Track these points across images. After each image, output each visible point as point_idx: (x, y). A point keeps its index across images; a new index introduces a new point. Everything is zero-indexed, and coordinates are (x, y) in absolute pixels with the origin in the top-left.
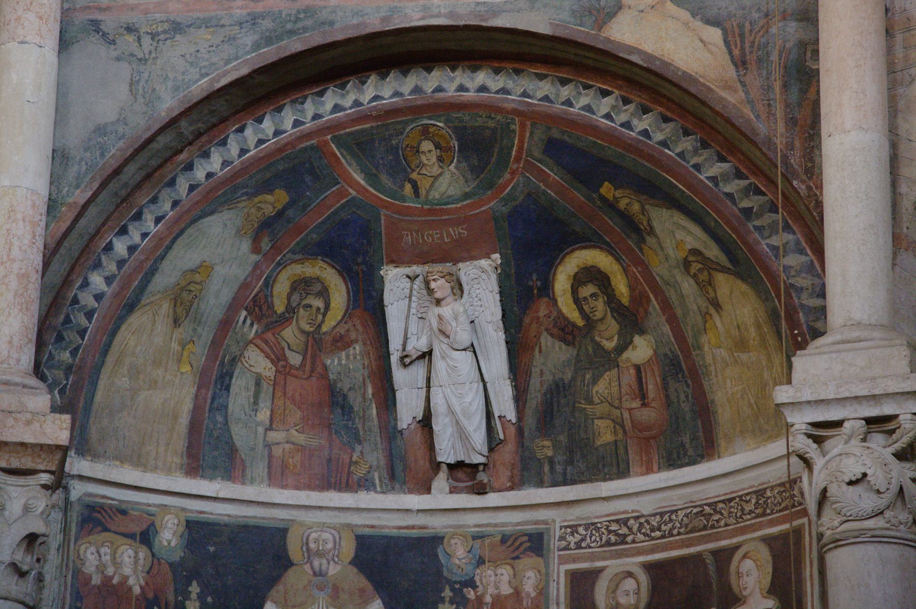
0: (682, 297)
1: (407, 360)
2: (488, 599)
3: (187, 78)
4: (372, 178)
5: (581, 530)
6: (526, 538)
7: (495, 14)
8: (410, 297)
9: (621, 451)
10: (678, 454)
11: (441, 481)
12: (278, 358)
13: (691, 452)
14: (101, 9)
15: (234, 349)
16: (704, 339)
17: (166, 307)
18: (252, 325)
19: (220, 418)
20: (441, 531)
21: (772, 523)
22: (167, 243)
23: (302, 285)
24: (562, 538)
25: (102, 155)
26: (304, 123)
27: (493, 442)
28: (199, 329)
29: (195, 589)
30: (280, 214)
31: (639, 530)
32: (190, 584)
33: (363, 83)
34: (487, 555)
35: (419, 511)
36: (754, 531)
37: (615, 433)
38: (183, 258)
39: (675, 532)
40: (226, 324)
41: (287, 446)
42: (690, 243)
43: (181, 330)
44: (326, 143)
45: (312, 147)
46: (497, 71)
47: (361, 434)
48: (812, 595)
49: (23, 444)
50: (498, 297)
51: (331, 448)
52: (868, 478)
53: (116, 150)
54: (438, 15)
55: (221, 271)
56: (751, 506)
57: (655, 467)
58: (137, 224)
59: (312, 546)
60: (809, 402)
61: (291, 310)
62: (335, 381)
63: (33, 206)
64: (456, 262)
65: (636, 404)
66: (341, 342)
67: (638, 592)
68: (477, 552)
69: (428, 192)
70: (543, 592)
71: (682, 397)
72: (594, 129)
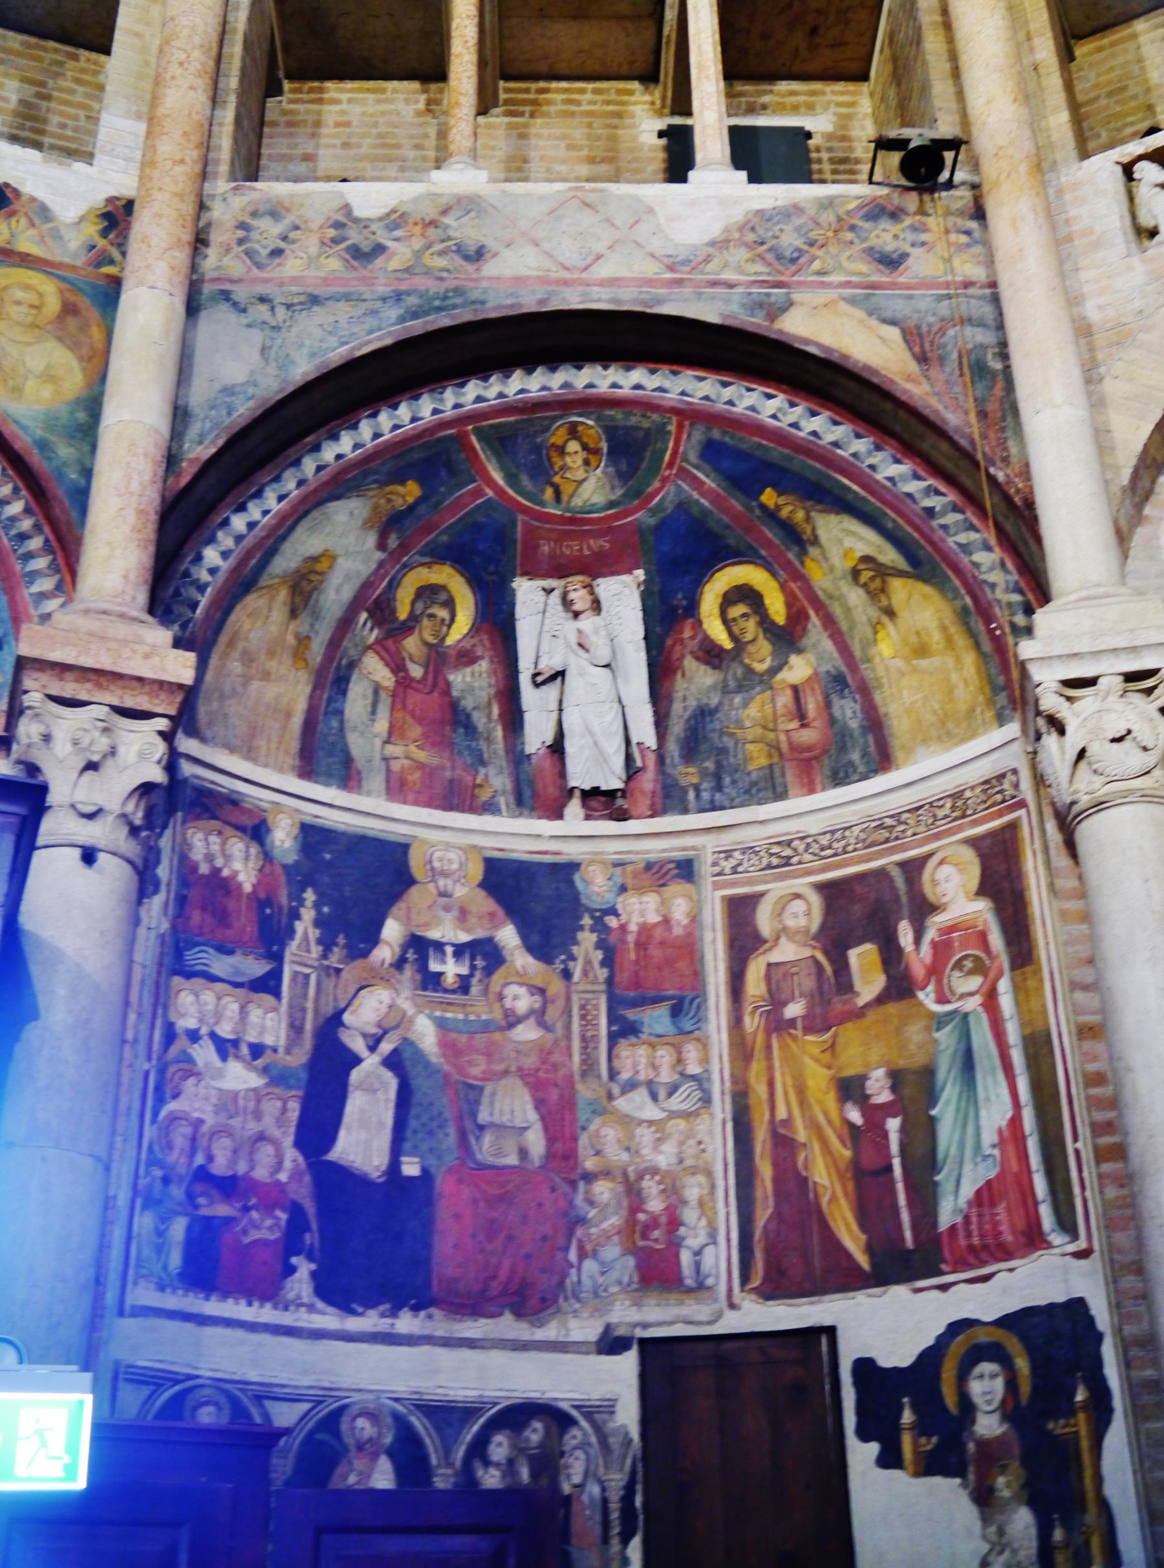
0: (848, 610)
1: (540, 679)
2: (633, 927)
3: (325, 346)
4: (511, 479)
5: (737, 855)
6: (672, 866)
7: (659, 302)
8: (544, 612)
9: (777, 773)
10: (846, 772)
11: (574, 808)
12: (398, 667)
13: (862, 769)
14: (232, 281)
15: (352, 653)
16: (873, 651)
17: (283, 594)
18: (372, 629)
19: (335, 723)
20: (576, 858)
21: (975, 823)
22: (289, 523)
23: (429, 593)
24: (715, 864)
25: (229, 414)
26: (442, 412)
27: (632, 770)
28: (317, 627)
29: (310, 896)
30: (411, 508)
31: (806, 850)
32: (304, 891)
33: (508, 377)
34: (629, 882)
35: (552, 837)
36: (955, 834)
37: (770, 756)
38: (304, 543)
39: (850, 848)
40: (346, 623)
41: (406, 762)
42: (861, 549)
43: (297, 622)
44: (466, 435)
45: (451, 438)
46: (653, 372)
47: (486, 756)
48: (1039, 887)
49: (140, 679)
50: (640, 614)
51: (453, 768)
52: (1133, 735)
53: (244, 410)
54: (599, 301)
55: (344, 565)
56: (946, 811)
57: (818, 787)
58: (256, 501)
59: (437, 864)
60: (1060, 657)
61: (414, 618)
62: (459, 699)
63: (156, 445)
64: (595, 575)
65: (794, 725)
66: (466, 658)
67: (808, 913)
68: (619, 880)
69: (572, 496)
70: (695, 919)
71: (849, 713)
72: (760, 429)
